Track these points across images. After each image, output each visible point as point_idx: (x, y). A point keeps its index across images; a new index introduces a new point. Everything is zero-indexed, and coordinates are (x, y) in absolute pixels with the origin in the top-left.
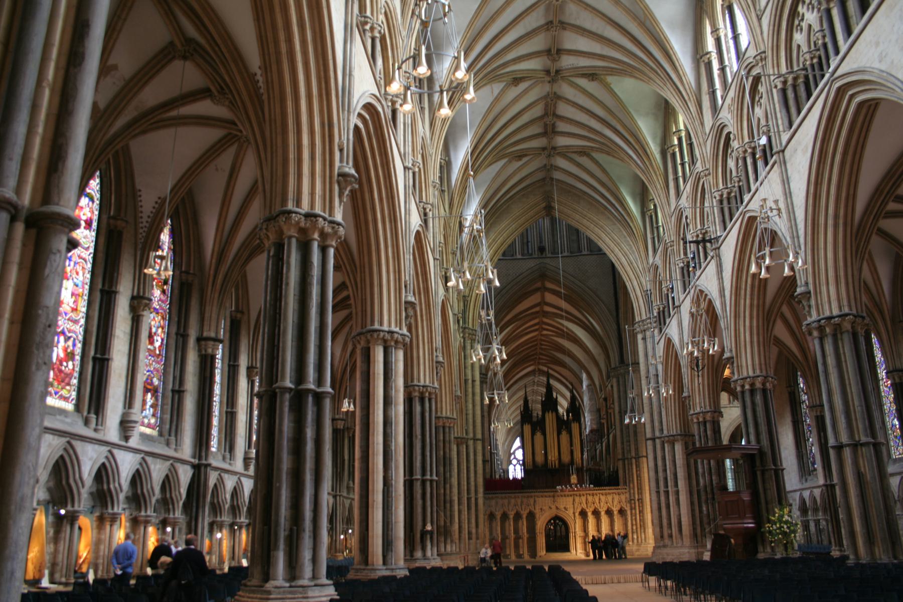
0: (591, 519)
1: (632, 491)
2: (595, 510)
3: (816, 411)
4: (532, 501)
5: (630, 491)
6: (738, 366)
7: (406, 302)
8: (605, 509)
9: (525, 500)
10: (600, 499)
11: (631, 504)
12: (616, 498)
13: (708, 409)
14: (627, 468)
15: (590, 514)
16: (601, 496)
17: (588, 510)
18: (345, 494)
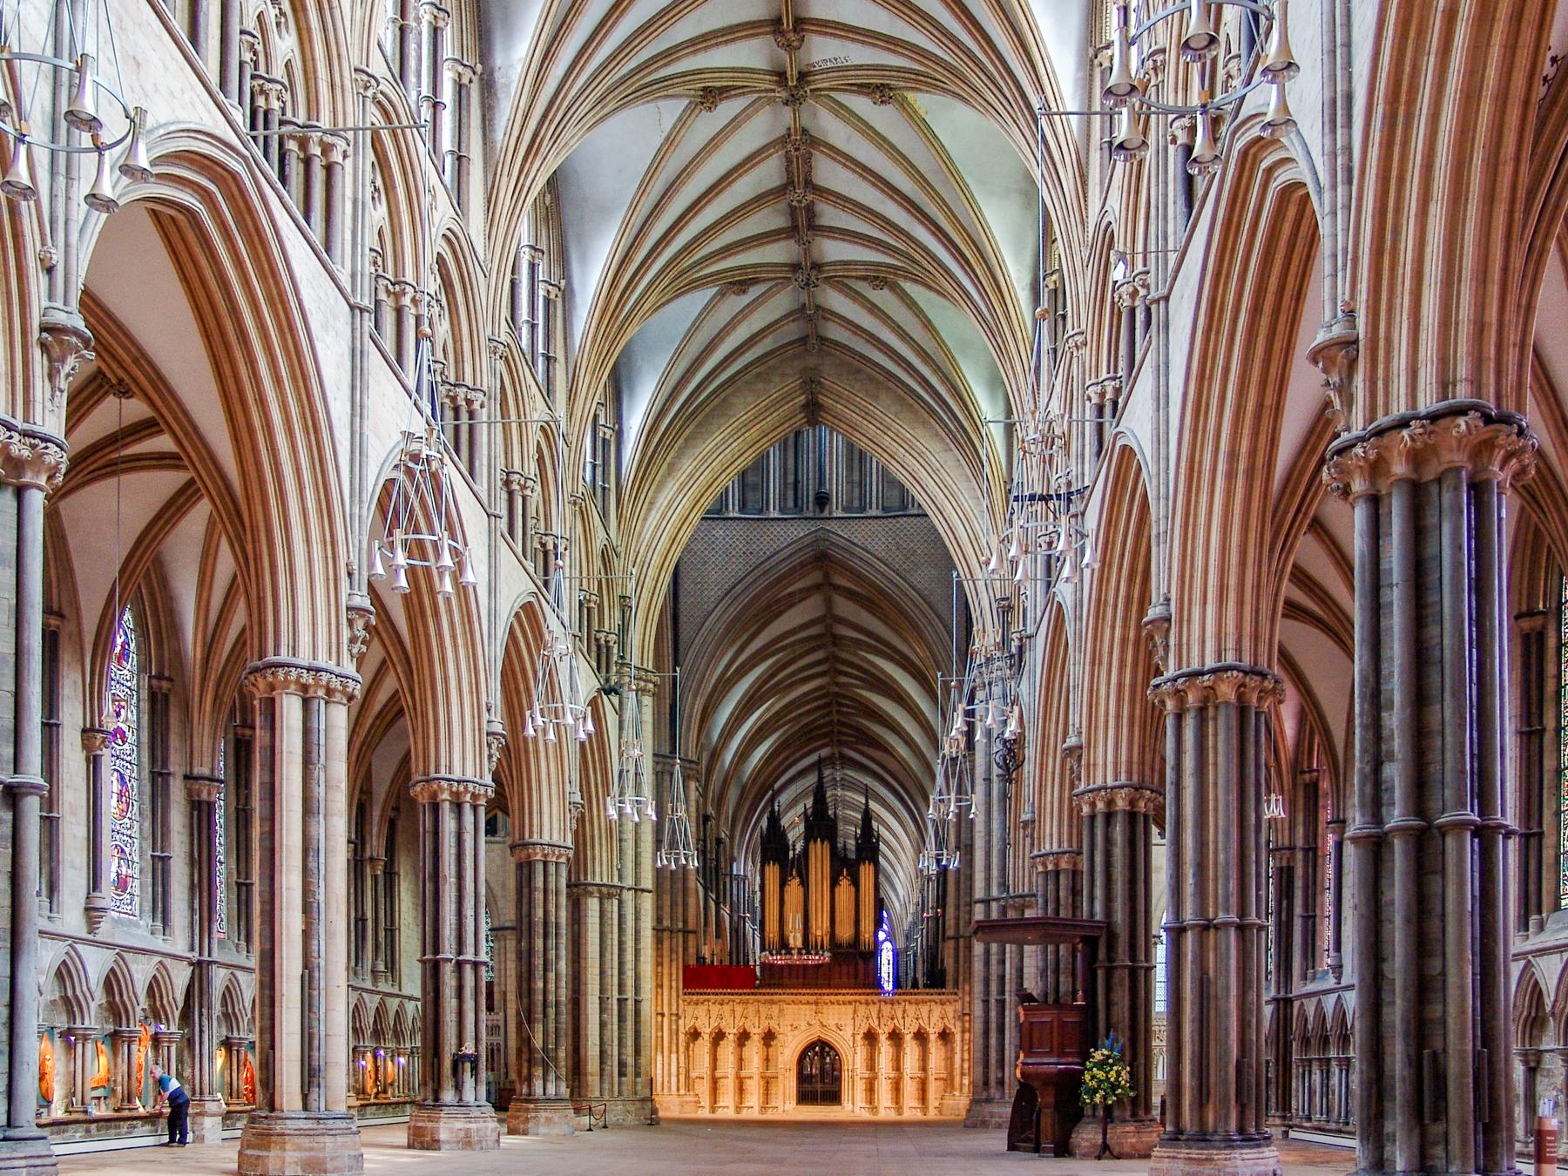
0: (885, 1049)
1: (967, 999)
2: (894, 1031)
3: (1281, 859)
4: (775, 1009)
5: (963, 999)
6: (1089, 765)
7: (348, 609)
8: (914, 1029)
9: (763, 1008)
10: (904, 1011)
11: (963, 1022)
12: (937, 1010)
13: (1065, 846)
14: (961, 954)
15: (883, 1038)
16: (908, 1007)
17: (880, 1031)
18: (368, 985)
